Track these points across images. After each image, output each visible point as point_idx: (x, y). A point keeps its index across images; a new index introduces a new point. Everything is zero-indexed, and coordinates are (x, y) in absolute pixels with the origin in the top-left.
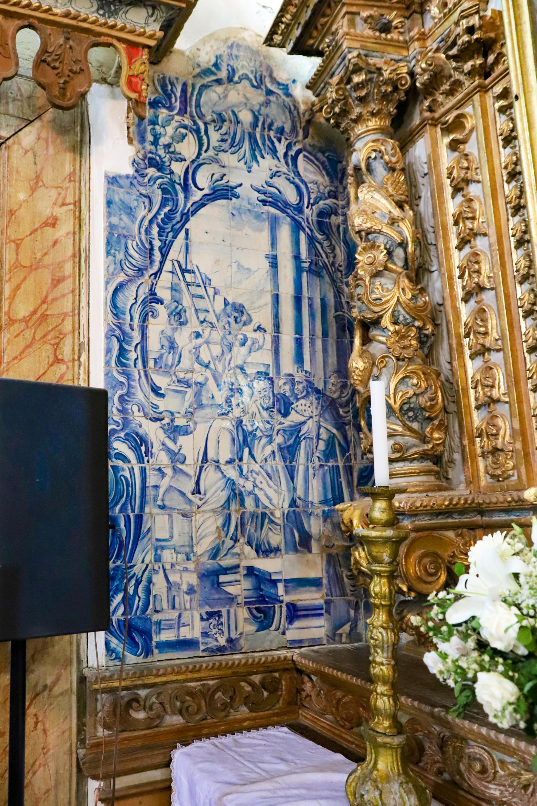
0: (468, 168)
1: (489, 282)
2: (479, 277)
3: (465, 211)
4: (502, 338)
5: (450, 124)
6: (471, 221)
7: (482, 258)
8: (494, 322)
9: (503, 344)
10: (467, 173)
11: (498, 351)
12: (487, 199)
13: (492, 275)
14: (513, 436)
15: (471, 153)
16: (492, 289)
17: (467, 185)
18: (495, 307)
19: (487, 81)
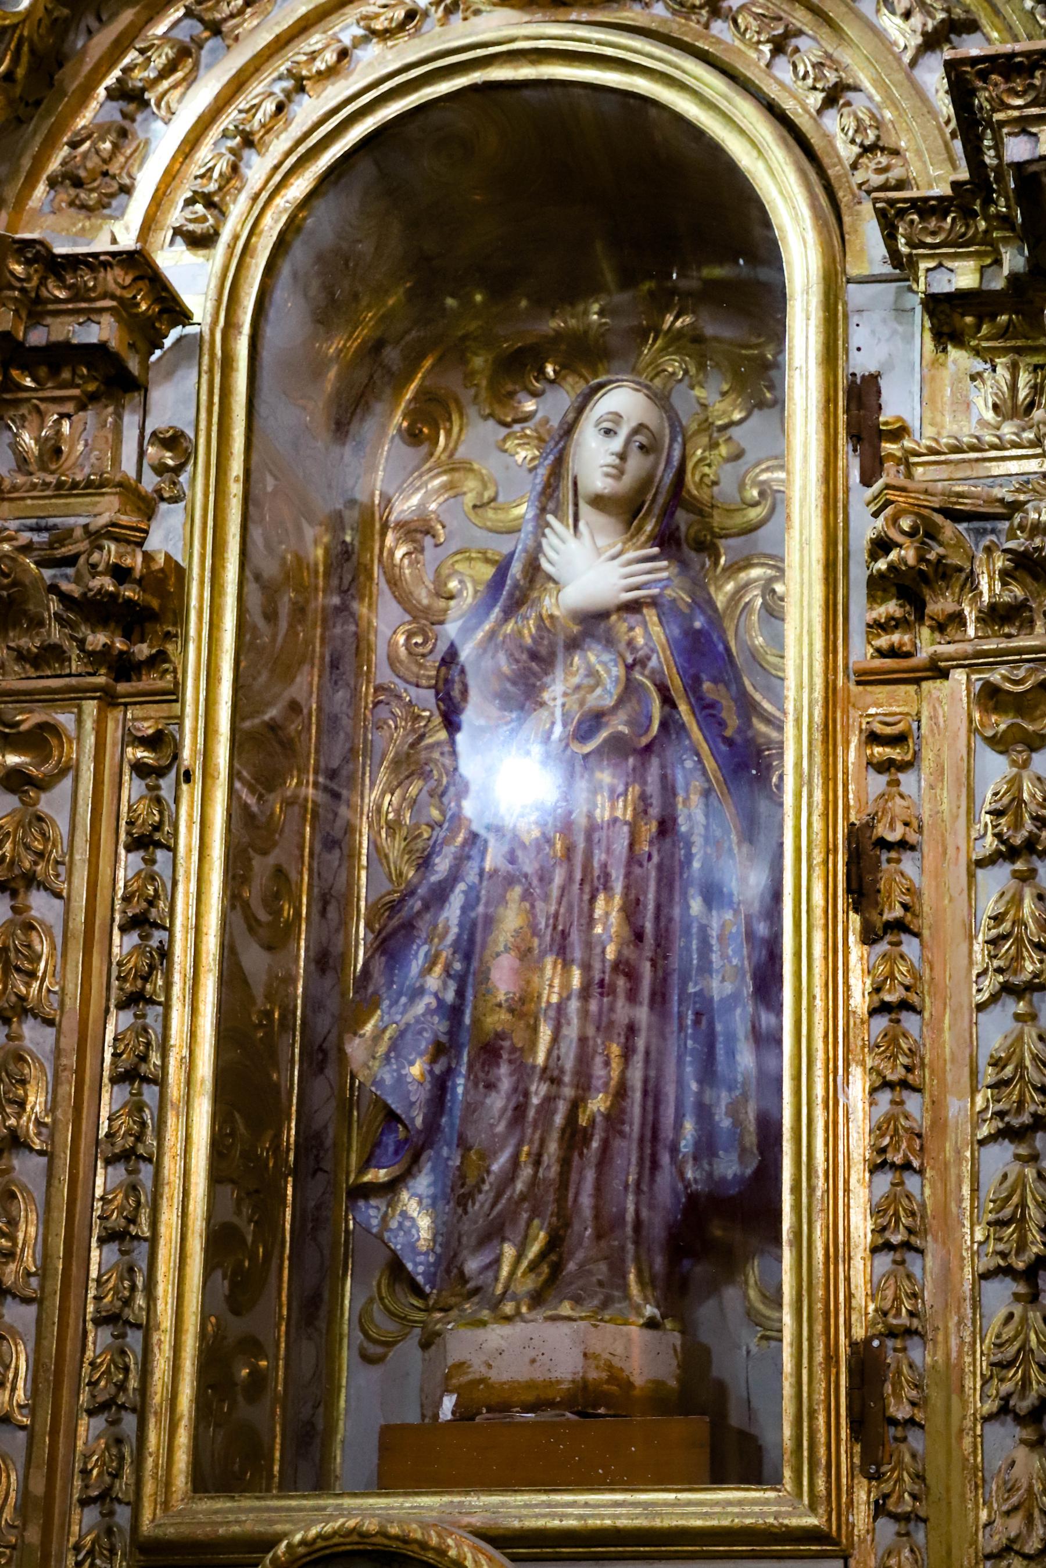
0: (41, 855)
1: (39, 1134)
2: (19, 1116)
3: (17, 951)
4: (44, 1272)
5: (19, 733)
6: (26, 979)
7: (31, 1071)
8: (32, 1230)
9: (42, 1287)
10: (36, 863)
11: (27, 1301)
12: (72, 944)
13: (48, 1120)
14: (21, 1509)
15: (53, 821)
16: (41, 1153)
17: (28, 887)
18: (39, 1195)
19: (122, 687)
